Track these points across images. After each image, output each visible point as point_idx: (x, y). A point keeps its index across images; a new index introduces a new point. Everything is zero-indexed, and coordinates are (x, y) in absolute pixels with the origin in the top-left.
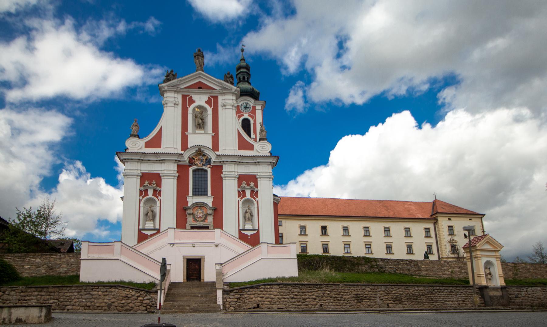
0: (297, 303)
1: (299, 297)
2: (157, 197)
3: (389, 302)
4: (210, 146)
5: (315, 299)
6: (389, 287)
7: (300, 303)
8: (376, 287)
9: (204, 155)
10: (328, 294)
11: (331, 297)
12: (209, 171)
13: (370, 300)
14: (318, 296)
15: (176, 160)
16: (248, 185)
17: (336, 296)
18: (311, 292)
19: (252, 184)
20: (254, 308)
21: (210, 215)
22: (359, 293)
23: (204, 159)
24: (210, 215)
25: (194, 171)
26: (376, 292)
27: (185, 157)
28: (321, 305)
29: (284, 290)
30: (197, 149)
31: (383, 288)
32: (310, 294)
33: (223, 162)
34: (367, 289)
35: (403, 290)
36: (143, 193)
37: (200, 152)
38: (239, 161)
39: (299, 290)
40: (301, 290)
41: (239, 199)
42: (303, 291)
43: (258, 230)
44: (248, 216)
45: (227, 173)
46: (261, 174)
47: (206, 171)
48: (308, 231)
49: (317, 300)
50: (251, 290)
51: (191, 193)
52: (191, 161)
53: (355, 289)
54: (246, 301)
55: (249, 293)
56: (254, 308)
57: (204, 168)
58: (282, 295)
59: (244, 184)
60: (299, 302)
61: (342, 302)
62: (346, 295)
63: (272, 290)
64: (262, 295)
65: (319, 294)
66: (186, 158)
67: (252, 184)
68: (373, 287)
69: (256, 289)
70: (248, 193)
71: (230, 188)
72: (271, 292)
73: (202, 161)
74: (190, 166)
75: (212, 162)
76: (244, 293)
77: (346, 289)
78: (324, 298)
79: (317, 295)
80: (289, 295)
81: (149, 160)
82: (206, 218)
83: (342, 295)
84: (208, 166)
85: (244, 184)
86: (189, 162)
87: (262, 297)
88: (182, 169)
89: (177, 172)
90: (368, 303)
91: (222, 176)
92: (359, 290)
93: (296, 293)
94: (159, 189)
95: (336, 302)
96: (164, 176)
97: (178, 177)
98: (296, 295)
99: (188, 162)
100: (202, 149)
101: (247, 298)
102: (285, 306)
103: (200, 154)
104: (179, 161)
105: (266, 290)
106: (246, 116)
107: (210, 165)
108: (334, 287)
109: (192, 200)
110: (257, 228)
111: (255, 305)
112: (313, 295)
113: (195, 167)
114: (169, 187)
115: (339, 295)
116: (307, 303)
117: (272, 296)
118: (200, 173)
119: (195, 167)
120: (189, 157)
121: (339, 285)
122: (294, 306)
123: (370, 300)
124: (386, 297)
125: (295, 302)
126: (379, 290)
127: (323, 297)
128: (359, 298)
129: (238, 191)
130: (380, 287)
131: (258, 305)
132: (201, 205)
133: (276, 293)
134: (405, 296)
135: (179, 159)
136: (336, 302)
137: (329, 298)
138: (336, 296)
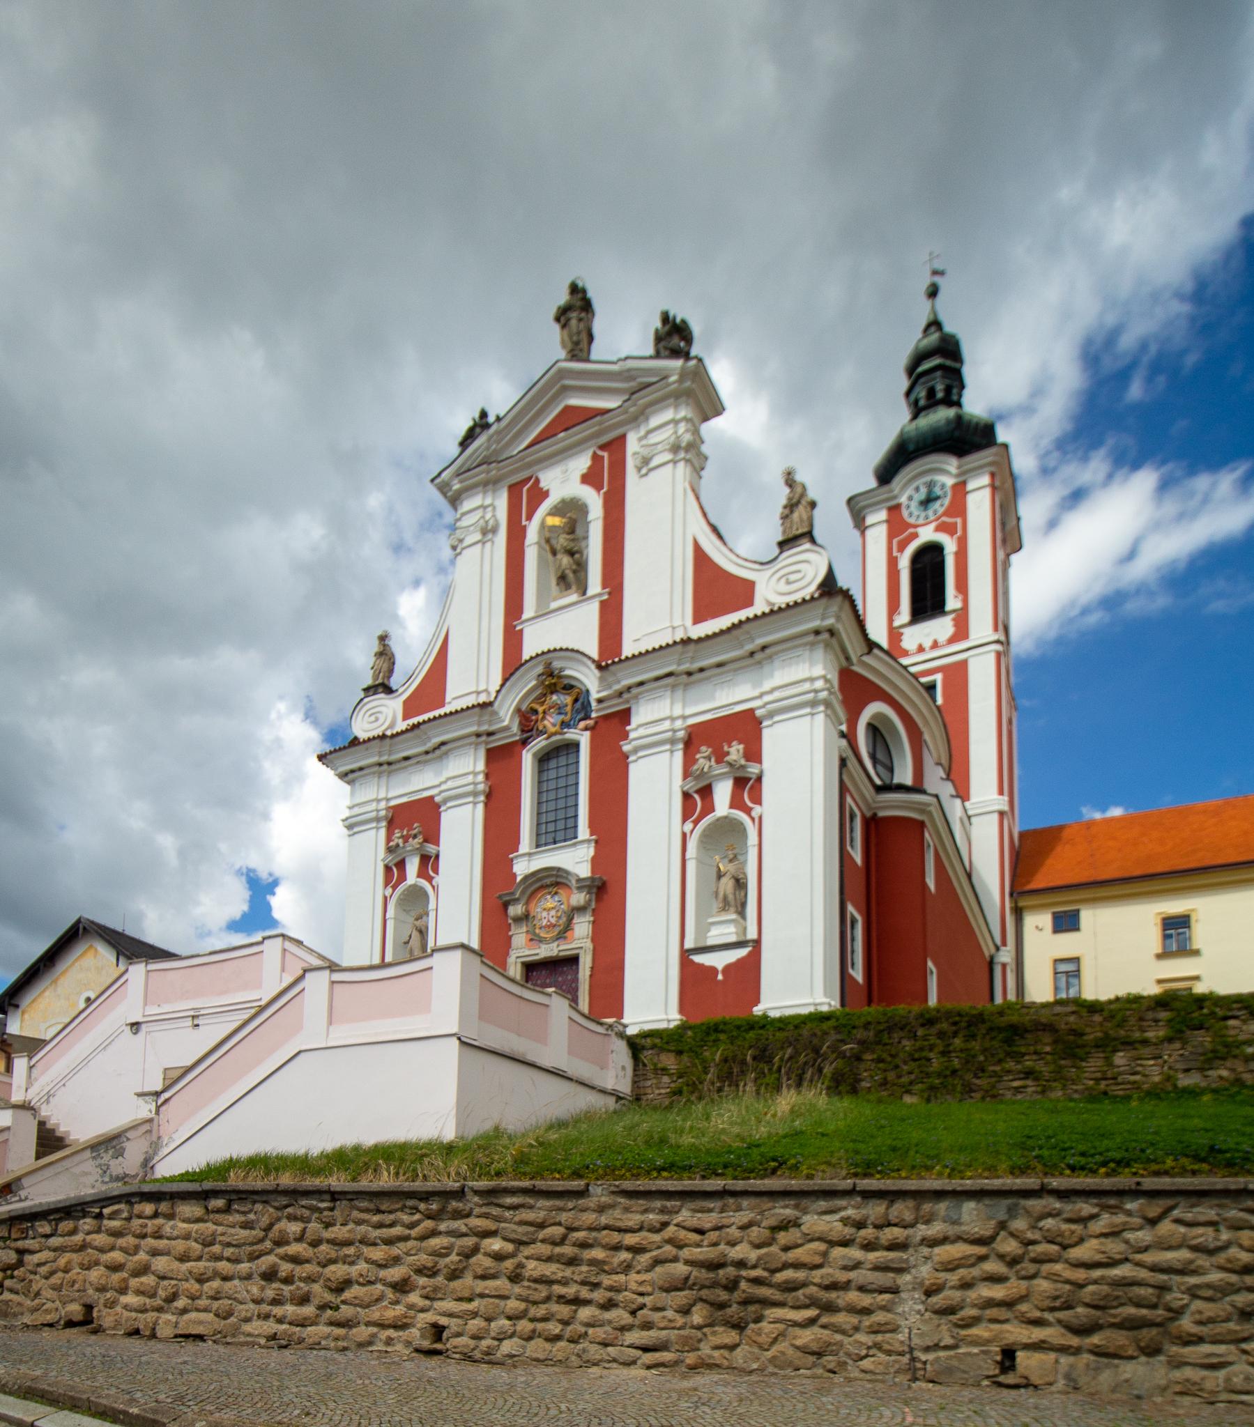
0: (290, 1309)
1: (309, 1268)
2: (430, 879)
3: (1016, 1333)
4: (593, 651)
5: (402, 1287)
6: (1035, 1204)
7: (308, 1310)
8: (902, 1210)
9: (568, 688)
10: (499, 1257)
11: (515, 1278)
12: (584, 740)
13: (830, 1308)
14: (432, 1272)
15: (478, 735)
16: (720, 756)
17: (550, 1270)
18: (389, 1242)
19: (735, 751)
20: (70, 1324)
21: (581, 909)
22: (736, 1253)
23: (568, 700)
24: (581, 909)
25: (543, 759)
26: (893, 1246)
27: (502, 714)
28: (438, 1331)
29: (230, 1228)
30: (540, 669)
31: (972, 1217)
32: (378, 1254)
33: (629, 688)
34: (816, 1221)
35: (1204, 1235)
36: (394, 872)
37: (553, 681)
38: (683, 664)
39: (314, 1226)
40: (328, 1225)
41: (689, 826)
42: (337, 1232)
43: (757, 943)
44: (736, 895)
45: (642, 732)
46: (767, 698)
47: (576, 746)
48: (1200, 935)
49: (414, 1298)
50: (66, 1225)
51: (525, 844)
52: (528, 722)
53: (708, 1220)
54: (38, 1283)
55: (55, 1241)
56: (70, 1324)
57: (571, 734)
58: (218, 1258)
59: (703, 761)
60: (304, 1300)
61: (585, 1313)
62: (627, 1268)
63: (168, 1227)
64: (117, 1256)
65: (438, 1254)
66: (506, 715)
67: (735, 751)
68: (875, 1210)
69: (87, 1223)
70: (723, 792)
71: (655, 783)
72: (158, 1235)
73: (560, 709)
74: (524, 742)
75: (594, 704)
76: (28, 1243)
77: (633, 1219)
78: (467, 1283)
79: (424, 1259)
80: (253, 1257)
81: (406, 758)
82: (568, 927)
83: (593, 1262)
84: (582, 724)
85: (703, 761)
86: (523, 731)
87: (115, 1268)
88: (501, 758)
89: (487, 776)
90: (806, 1337)
91: (626, 748)
92: (738, 1234)
93: (294, 1248)
94: (431, 849)
95: (541, 1311)
96: (445, 801)
97: (489, 796)
98: (296, 1260)
99: (515, 728)
100: (557, 664)
101: (43, 1270)
102: (221, 1324)
103: (552, 689)
104: (490, 734)
105: (136, 1223)
106: (927, 534)
107: (587, 717)
108: (540, 1209)
109: (522, 868)
110: (752, 934)
111: (75, 1309)
112: (396, 1260)
113: (539, 743)
114: (462, 833)
115: (572, 1262)
116: (346, 1311)
117: (160, 1264)
118: (563, 761)
119: (539, 743)
120: (518, 710)
121: (582, 1193)
122: (271, 1327)
123: (830, 1308)
124: (998, 1292)
125: (276, 1302)
126: (936, 1229)
127: (454, 1275)
128: (730, 1297)
129: (686, 796)
130: (942, 1207)
131: (89, 1308)
132: (552, 880)
133: (180, 1246)
134: (1225, 1290)
135: (485, 728)
136: (541, 1311)
137: (501, 1284)
138: (550, 1270)
